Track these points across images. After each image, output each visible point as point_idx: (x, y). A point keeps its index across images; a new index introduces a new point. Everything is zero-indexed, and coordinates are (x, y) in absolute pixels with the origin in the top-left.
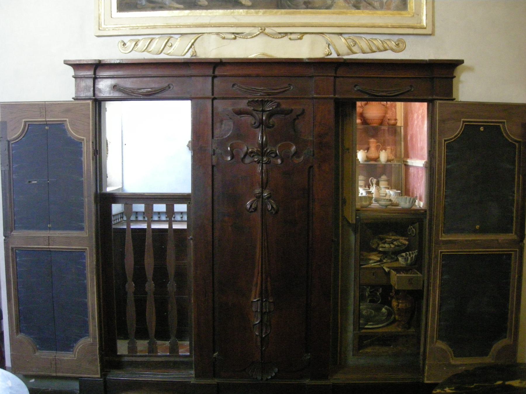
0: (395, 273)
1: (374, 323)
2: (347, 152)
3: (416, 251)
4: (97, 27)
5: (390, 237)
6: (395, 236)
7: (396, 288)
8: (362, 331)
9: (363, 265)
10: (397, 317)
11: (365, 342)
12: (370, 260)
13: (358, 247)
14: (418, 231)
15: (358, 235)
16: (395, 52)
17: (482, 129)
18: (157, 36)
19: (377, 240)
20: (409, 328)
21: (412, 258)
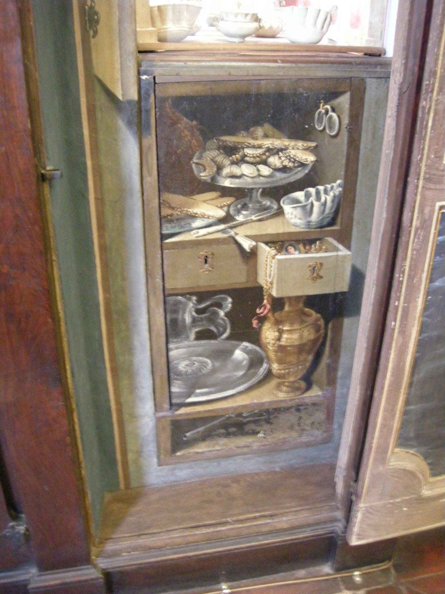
0: (273, 252)
1: (212, 389)
3: (339, 182)
5: (256, 143)
6: (273, 137)
7: (274, 293)
10: (275, 367)
11: (188, 434)
12: (194, 217)
13: (152, 179)
14: (346, 121)
15: (150, 140)
19: (213, 153)
20: (309, 387)
21: (325, 204)
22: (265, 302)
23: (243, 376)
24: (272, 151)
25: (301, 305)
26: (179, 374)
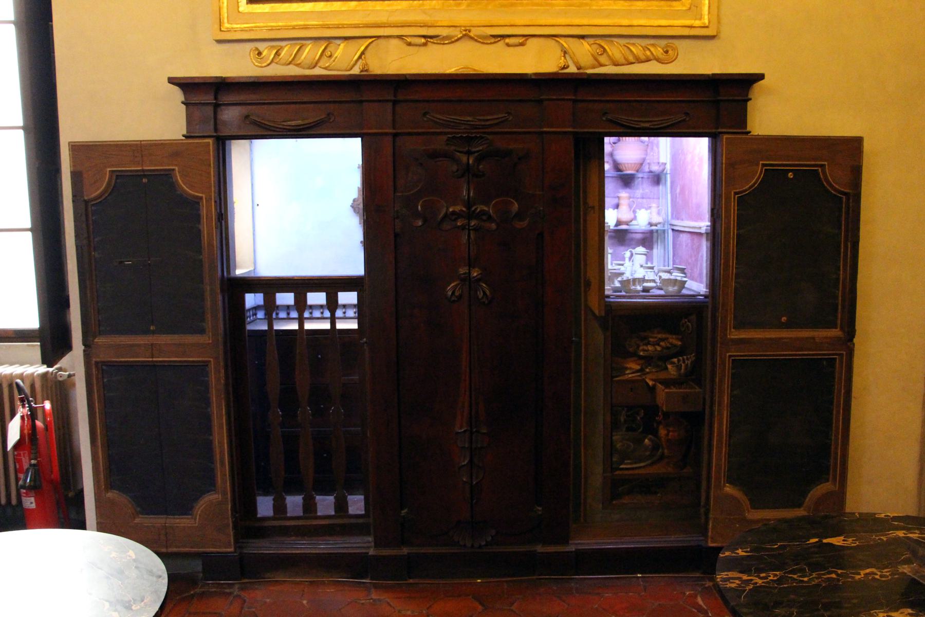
0: (663, 388)
2: (592, 211)
3: (693, 354)
4: (217, 26)
5: (655, 335)
7: (664, 410)
8: (615, 473)
9: (617, 377)
10: (666, 451)
12: (627, 368)
16: (662, 63)
17: (790, 175)
18: (309, 42)
21: (688, 364)
22: (660, 414)
24: (662, 340)
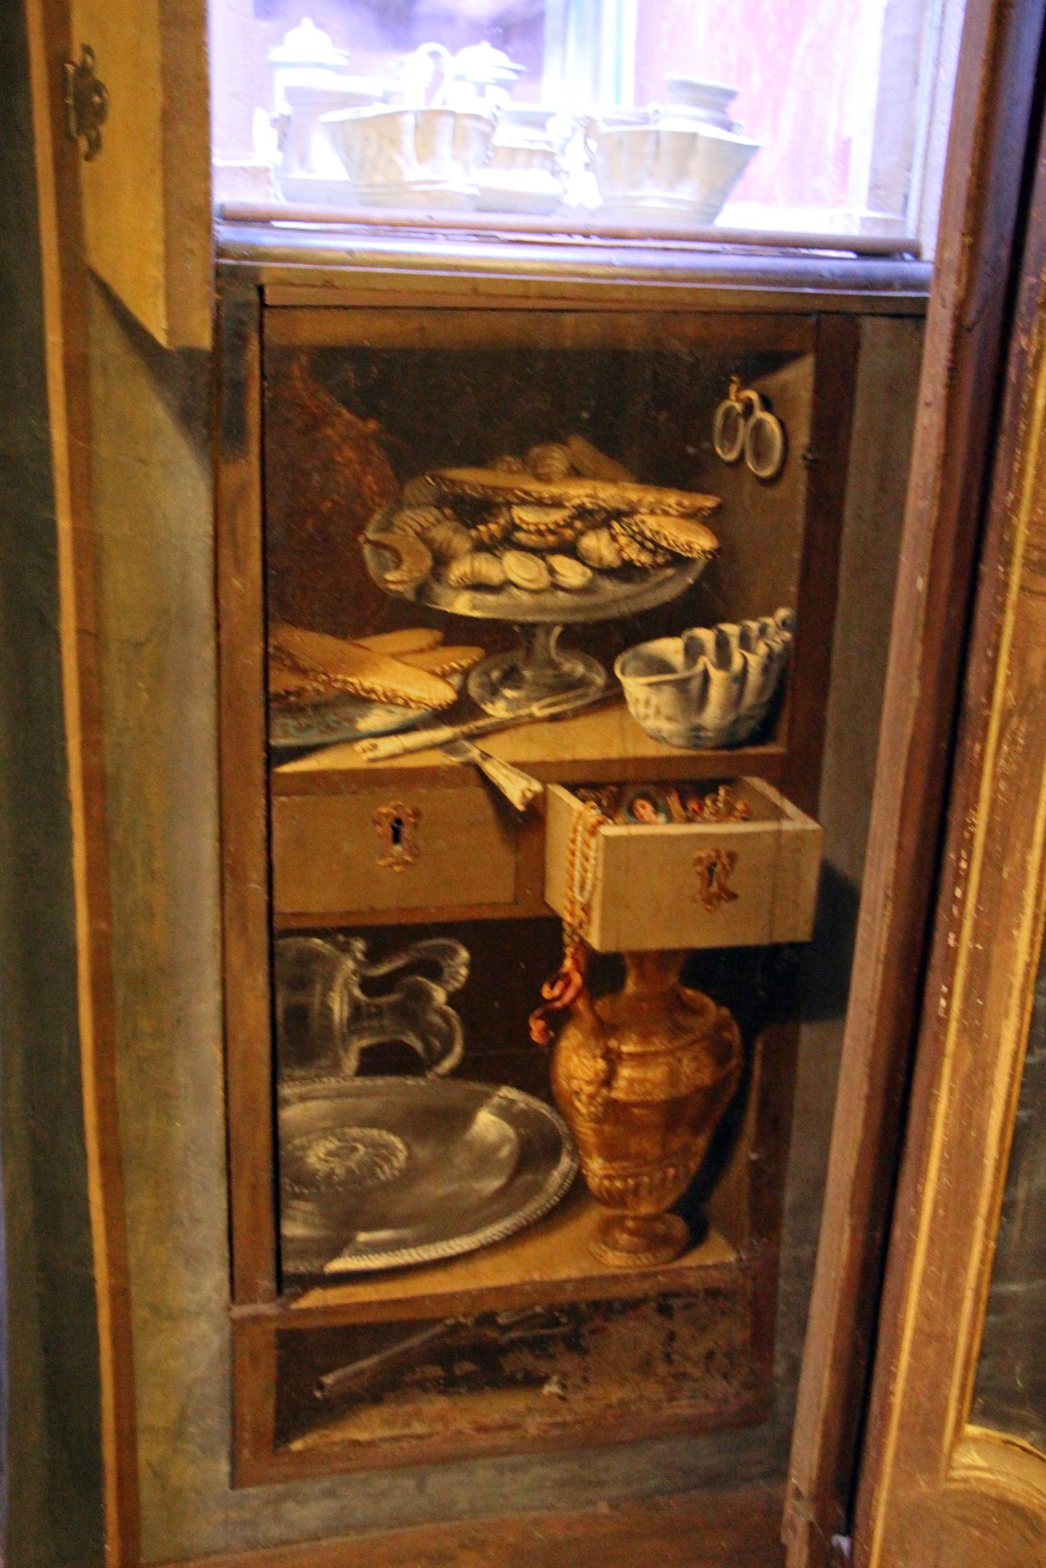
0: (593, 814)
1: (405, 1233)
3: (782, 613)
5: (547, 491)
6: (596, 476)
7: (595, 941)
8: (304, 1303)
10: (596, 1166)
11: (328, 1380)
12: (364, 701)
14: (802, 438)
19: (426, 516)
20: (697, 1238)
21: (742, 678)
22: (568, 963)
23: (501, 1192)
25: (673, 979)
26: (307, 1179)
